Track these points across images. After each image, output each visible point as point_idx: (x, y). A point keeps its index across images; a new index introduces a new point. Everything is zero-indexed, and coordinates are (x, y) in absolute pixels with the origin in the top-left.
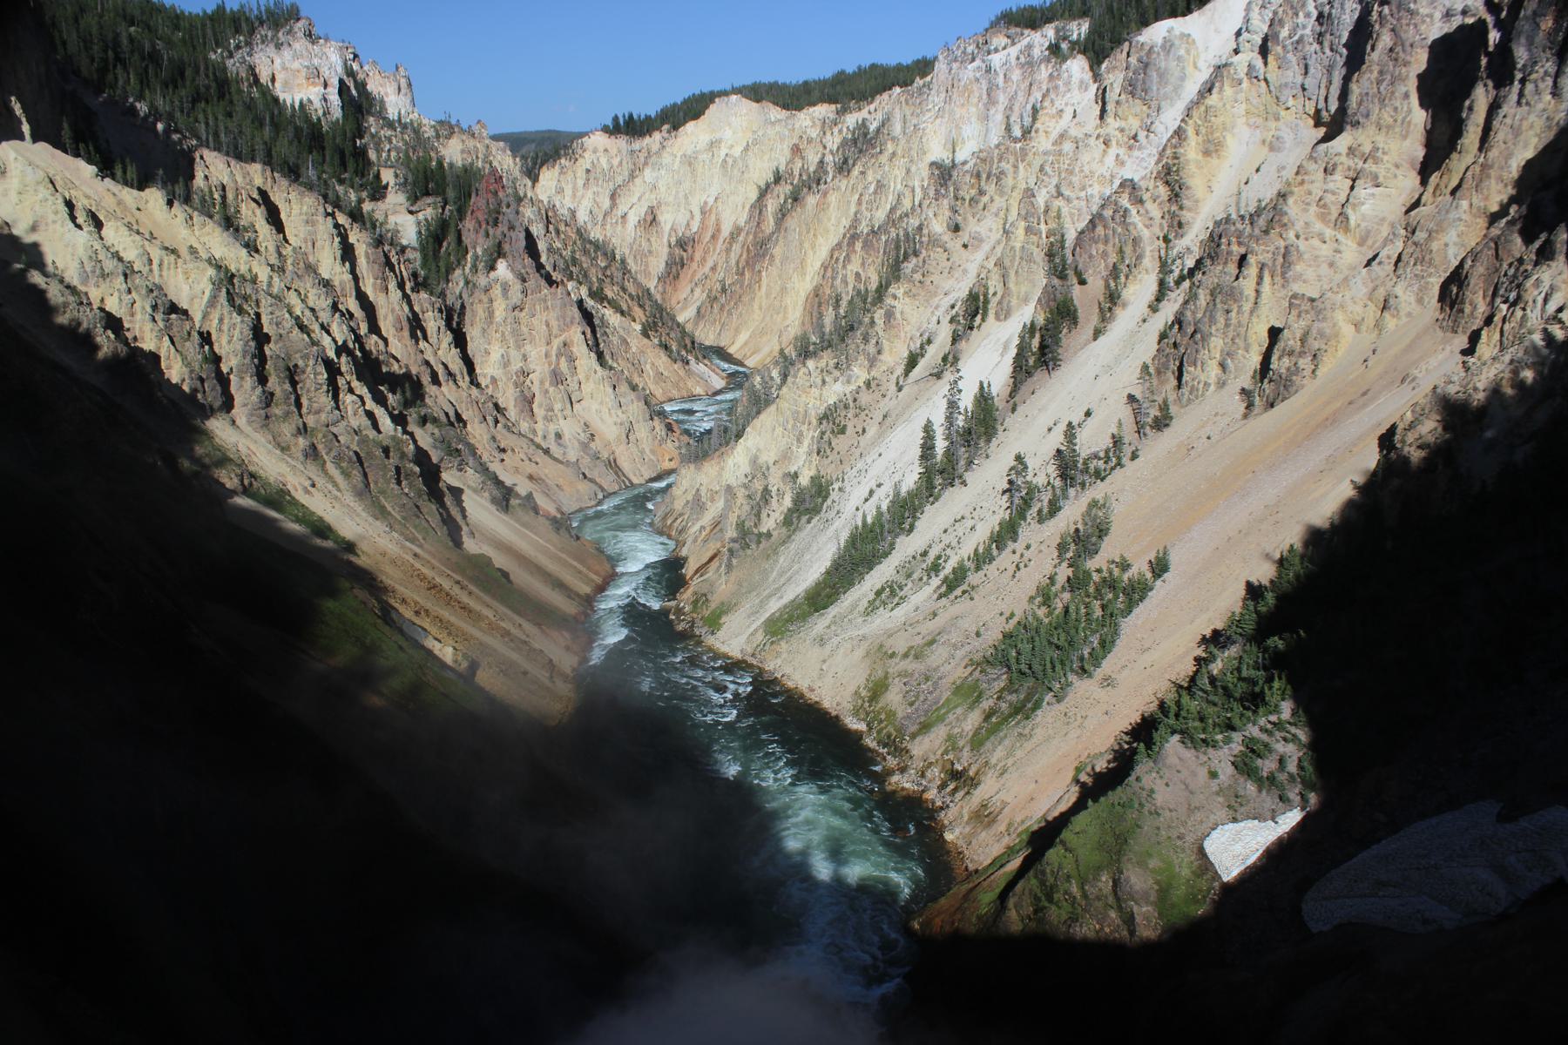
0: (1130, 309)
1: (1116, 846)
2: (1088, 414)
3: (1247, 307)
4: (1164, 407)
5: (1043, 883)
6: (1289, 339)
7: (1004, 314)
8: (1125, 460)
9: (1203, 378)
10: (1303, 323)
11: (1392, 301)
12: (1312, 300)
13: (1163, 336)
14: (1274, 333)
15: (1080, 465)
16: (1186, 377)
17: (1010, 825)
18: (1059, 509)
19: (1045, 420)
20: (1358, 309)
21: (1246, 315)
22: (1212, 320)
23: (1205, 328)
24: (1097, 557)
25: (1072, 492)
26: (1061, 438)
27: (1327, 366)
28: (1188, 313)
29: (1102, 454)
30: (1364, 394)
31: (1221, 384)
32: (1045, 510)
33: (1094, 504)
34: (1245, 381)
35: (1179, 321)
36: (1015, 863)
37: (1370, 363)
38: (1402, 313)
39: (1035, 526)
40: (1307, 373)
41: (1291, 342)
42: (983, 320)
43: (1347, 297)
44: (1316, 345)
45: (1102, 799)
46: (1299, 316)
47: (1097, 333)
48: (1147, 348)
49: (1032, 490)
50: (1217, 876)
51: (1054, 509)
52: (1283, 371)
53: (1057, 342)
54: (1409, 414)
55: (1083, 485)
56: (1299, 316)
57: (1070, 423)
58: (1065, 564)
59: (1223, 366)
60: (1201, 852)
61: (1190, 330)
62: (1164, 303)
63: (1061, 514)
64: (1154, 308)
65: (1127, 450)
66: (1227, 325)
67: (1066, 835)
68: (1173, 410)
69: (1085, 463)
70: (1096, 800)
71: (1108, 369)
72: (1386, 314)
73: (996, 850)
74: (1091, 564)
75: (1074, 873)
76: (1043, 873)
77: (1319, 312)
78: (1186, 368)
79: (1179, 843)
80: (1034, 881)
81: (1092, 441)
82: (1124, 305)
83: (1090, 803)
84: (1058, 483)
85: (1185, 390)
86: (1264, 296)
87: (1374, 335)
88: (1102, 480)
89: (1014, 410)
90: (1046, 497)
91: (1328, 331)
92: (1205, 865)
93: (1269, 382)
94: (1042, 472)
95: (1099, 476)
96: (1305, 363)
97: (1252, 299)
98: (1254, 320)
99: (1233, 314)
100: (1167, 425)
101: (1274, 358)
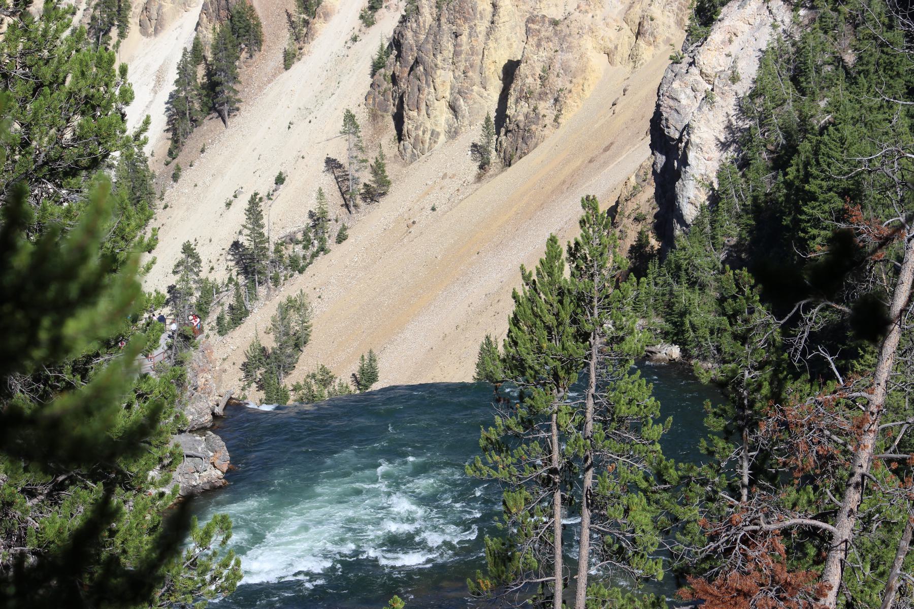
0: (335, 20)
2: (280, 180)
3: (482, 27)
4: (378, 169)
6: (528, 77)
7: (153, 24)
8: (330, 243)
9: (428, 125)
10: (543, 54)
11: (647, 25)
12: (555, 23)
13: (377, 66)
14: (510, 70)
15: (271, 254)
16: (408, 126)
18: (247, 313)
19: (221, 190)
20: (611, 33)
21: (482, 37)
22: (437, 48)
23: (428, 59)
24: (295, 373)
25: (262, 291)
26: (243, 218)
27: (573, 110)
28: (409, 34)
29: (300, 237)
30: (607, 149)
31: (453, 134)
32: (227, 318)
33: (294, 306)
34: (475, 133)
35: (397, 43)
37: (617, 108)
38: (660, 40)
39: (215, 338)
40: (549, 121)
41: (530, 80)
42: (122, 35)
43: (598, 18)
44: (559, 83)
46: (539, 45)
47: (289, 59)
48: (357, 83)
49: (209, 291)
51: (238, 314)
52: (521, 118)
53: (235, 79)
54: (633, 181)
55: (276, 280)
56: (539, 45)
57: (254, 202)
58: (254, 385)
59: (453, 108)
61: (411, 60)
62: (380, 11)
63: (249, 321)
64: (367, 20)
65: (333, 229)
66: (456, 54)
68: (391, 171)
69: (277, 251)
71: (307, 113)
72: (641, 42)
74: (288, 382)
77: (562, 40)
78: (411, 114)
81: (284, 219)
82: (327, 16)
84: (241, 280)
85: (407, 143)
86: (502, 11)
87: (629, 68)
88: (301, 271)
89: (175, 178)
90: (229, 299)
91: (574, 64)
93: (506, 135)
94: (218, 268)
95: (297, 266)
96: (545, 107)
97: (489, 17)
98: (491, 44)
99: (464, 38)
100: (384, 194)
101: (511, 100)
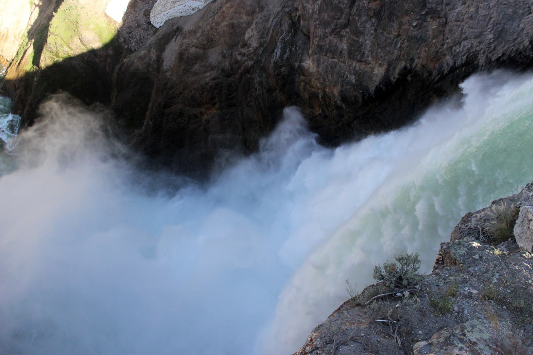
1: (75, 26)
5: (52, 52)
17: (15, 37)
36: (31, 51)
45: (59, 10)
50: (115, 22)
60: (106, 16)
67: (51, 29)
70: (56, 11)
73: (15, 49)
75: (63, 43)
76: (50, 48)
79: (97, 15)
80: (48, 53)
83: (54, 14)
92: (110, 20)
